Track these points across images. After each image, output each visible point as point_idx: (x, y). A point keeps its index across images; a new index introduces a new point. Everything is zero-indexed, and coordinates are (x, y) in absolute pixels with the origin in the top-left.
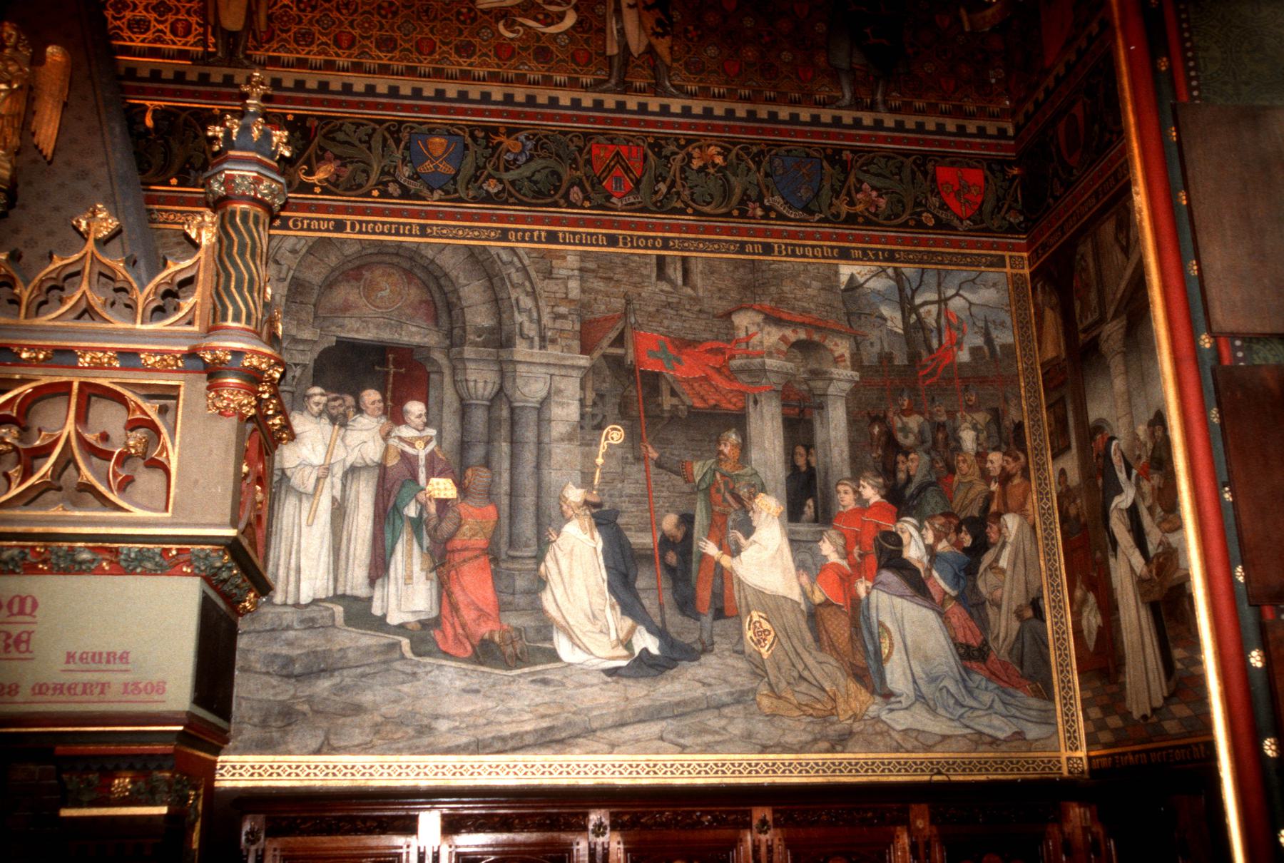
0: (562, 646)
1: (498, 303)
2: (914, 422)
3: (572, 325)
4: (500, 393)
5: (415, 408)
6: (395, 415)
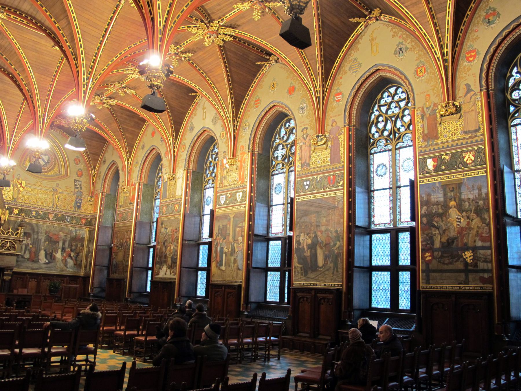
0: (40, 262)
1: (38, 229)
2: (74, 244)
3: (45, 232)
4: (37, 238)
5: (29, 239)
6: (27, 239)
